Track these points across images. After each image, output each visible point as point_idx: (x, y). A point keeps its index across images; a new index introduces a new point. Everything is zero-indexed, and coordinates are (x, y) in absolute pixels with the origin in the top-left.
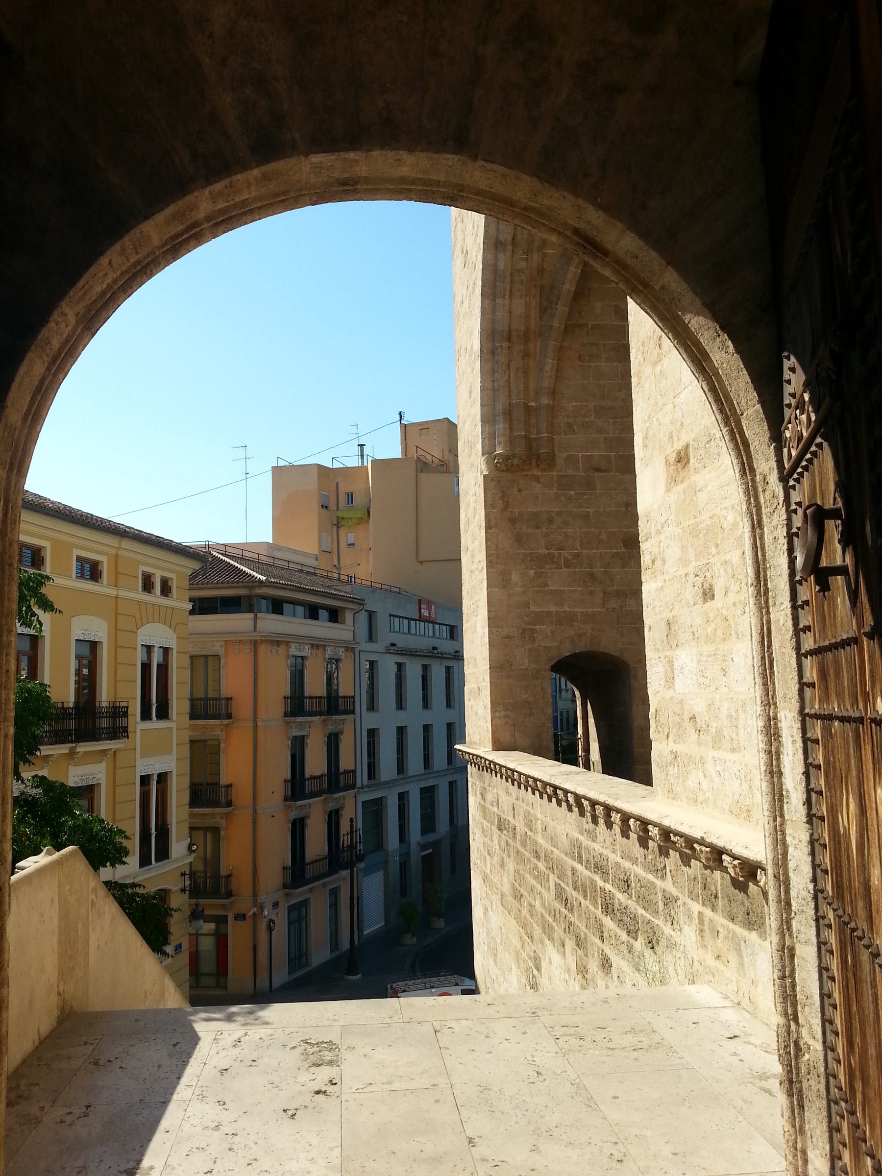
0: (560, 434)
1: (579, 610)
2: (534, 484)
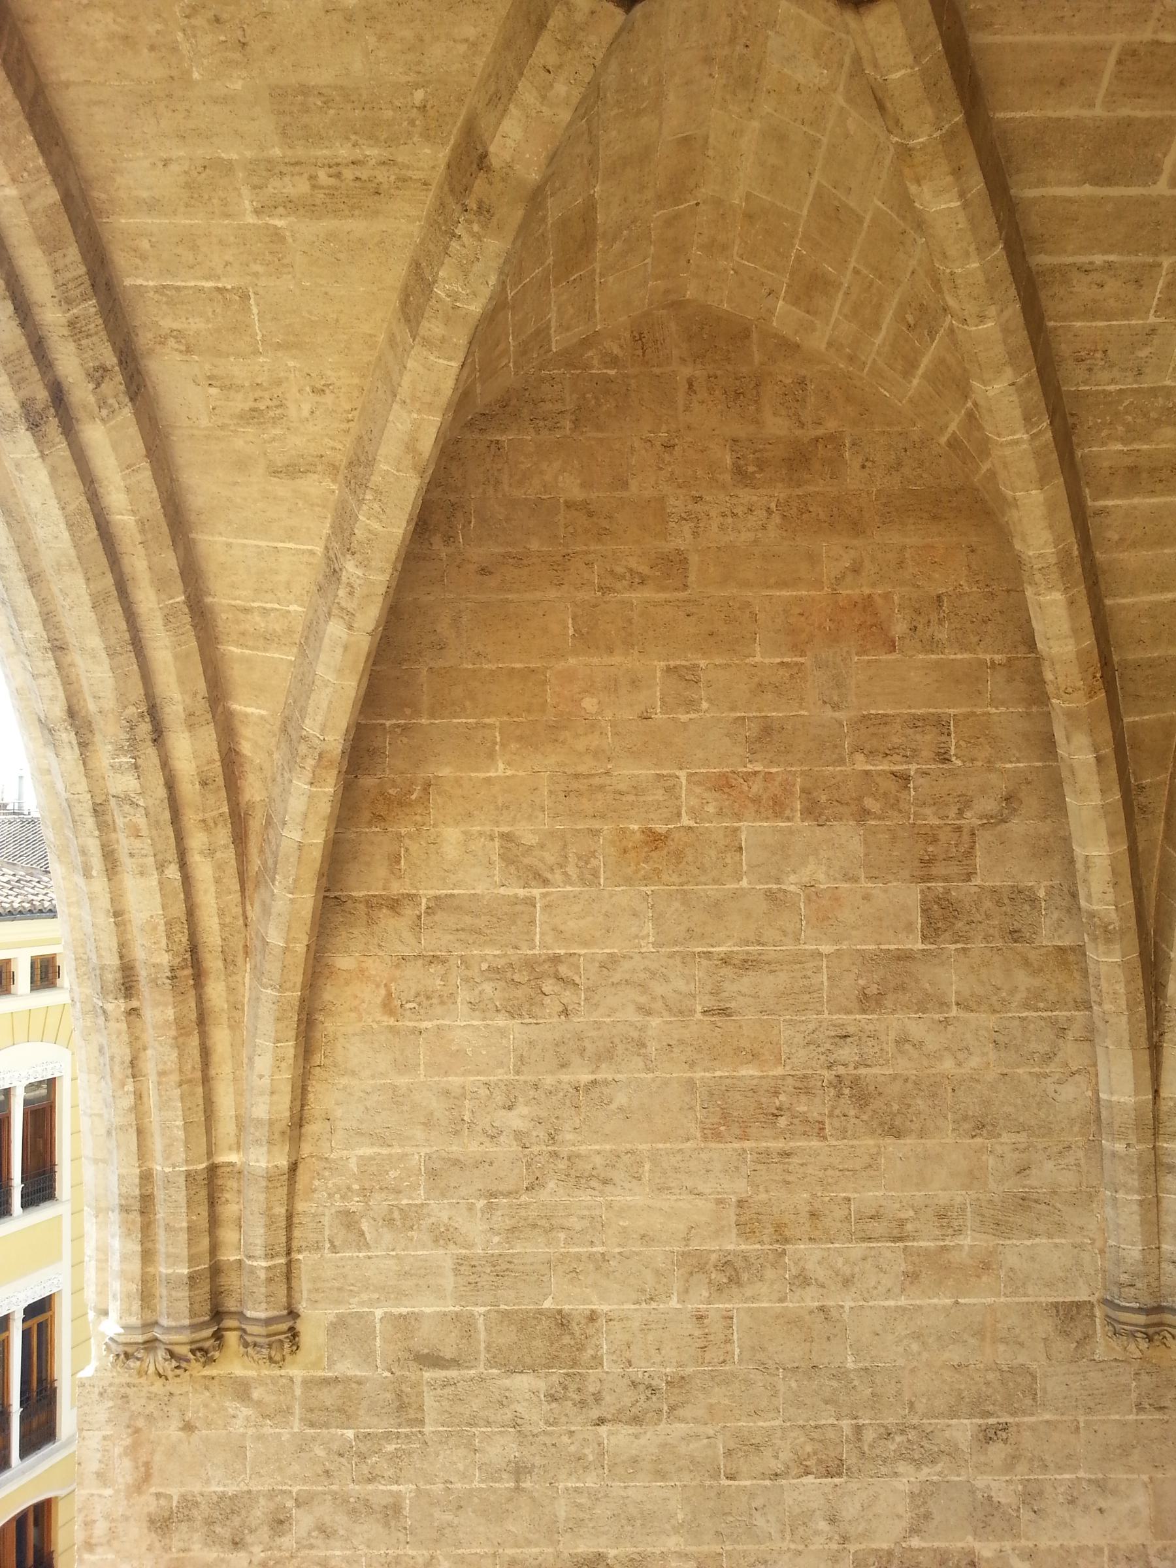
0: (317, 1247)
2: (231, 1406)
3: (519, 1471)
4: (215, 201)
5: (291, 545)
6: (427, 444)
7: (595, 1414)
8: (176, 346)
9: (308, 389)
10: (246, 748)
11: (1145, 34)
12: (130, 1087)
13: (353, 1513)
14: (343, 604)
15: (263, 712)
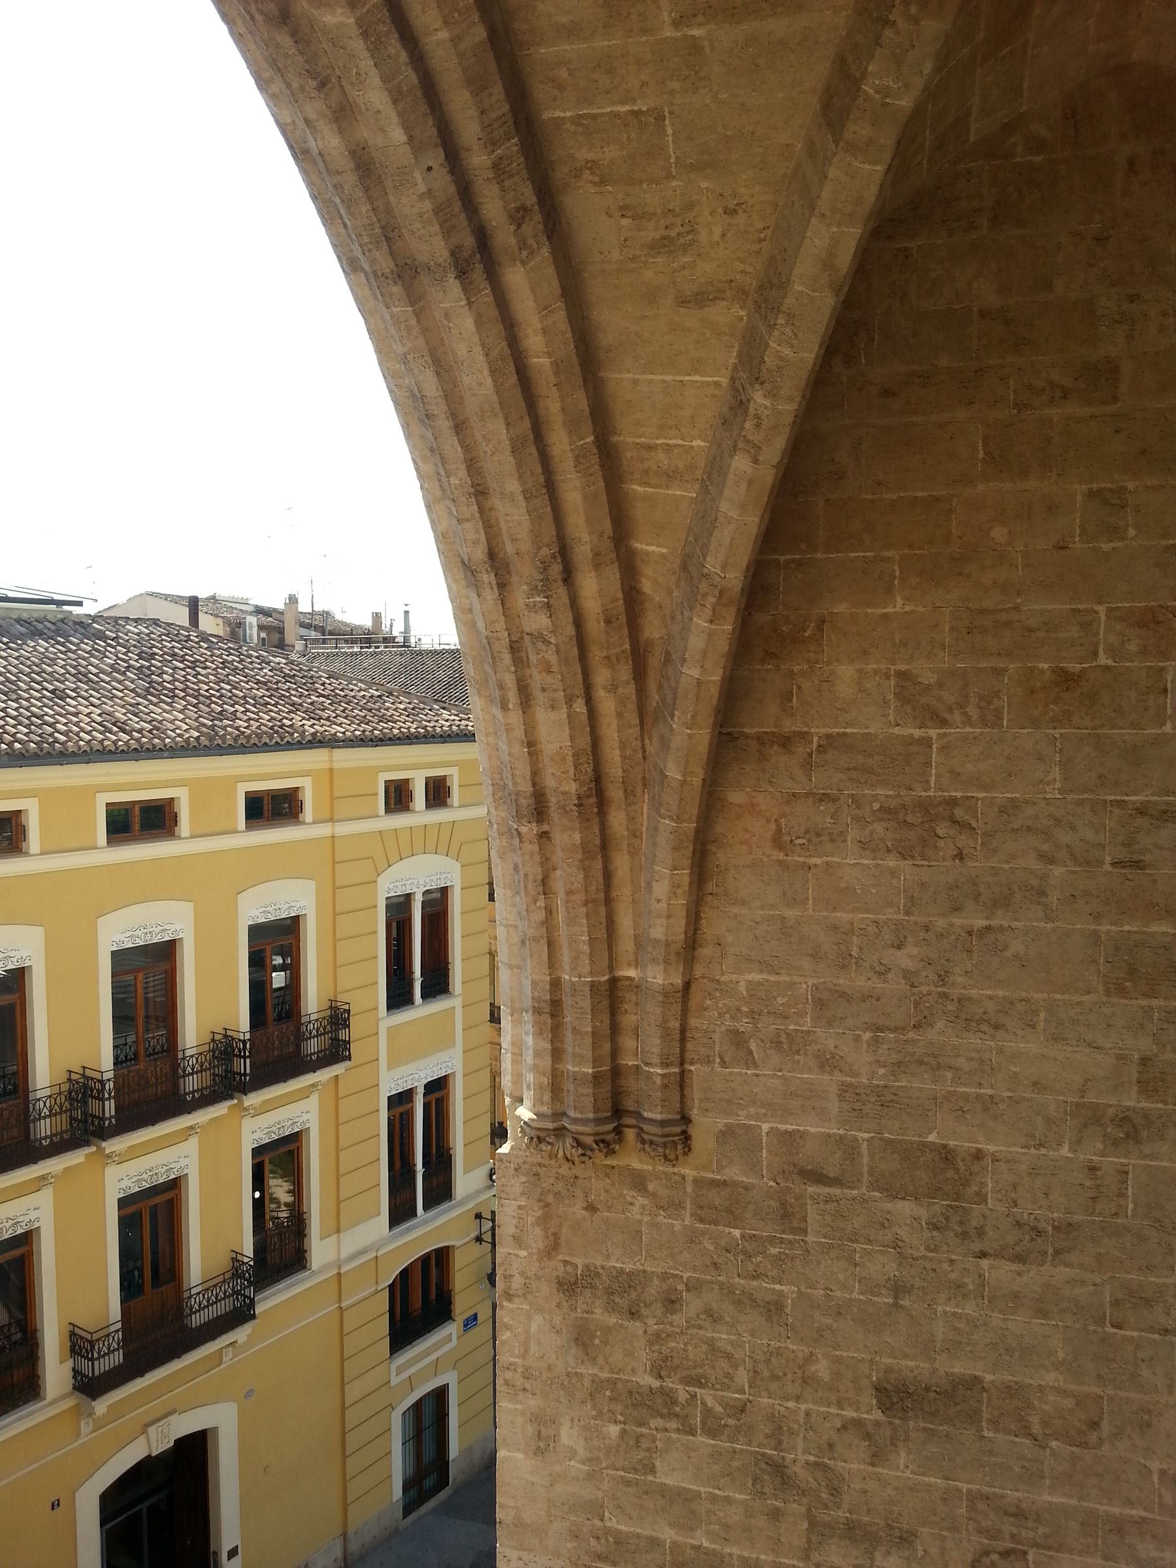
0: (708, 1061)
1: (736, 1551)
2: (629, 1194)
3: (898, 1289)
4: (634, 17)
5: (697, 378)
6: (845, 260)
7: (977, 1246)
8: (590, 178)
9: (720, 210)
10: (647, 586)
12: (541, 903)
13: (738, 1303)
14: (750, 437)
15: (664, 550)
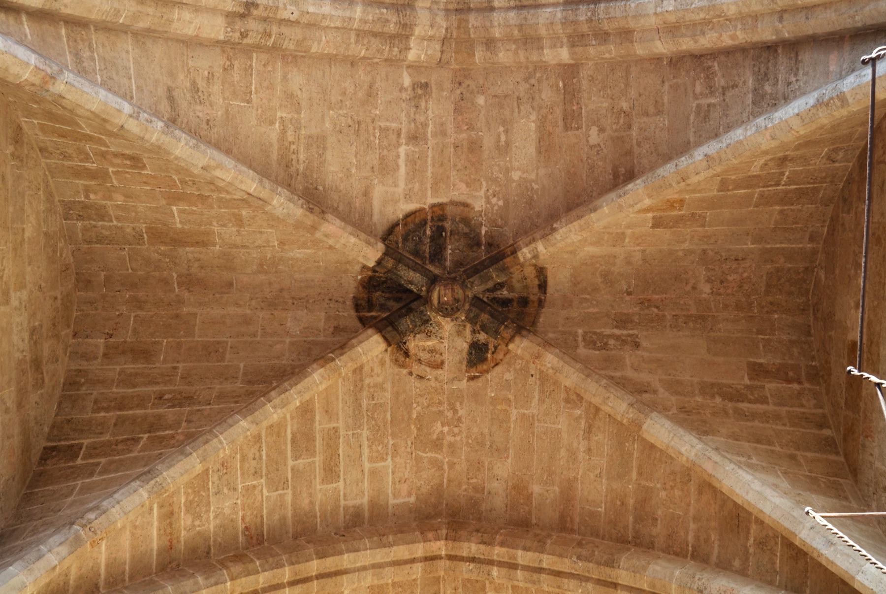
5: (134, 88)
11: (342, 432)
